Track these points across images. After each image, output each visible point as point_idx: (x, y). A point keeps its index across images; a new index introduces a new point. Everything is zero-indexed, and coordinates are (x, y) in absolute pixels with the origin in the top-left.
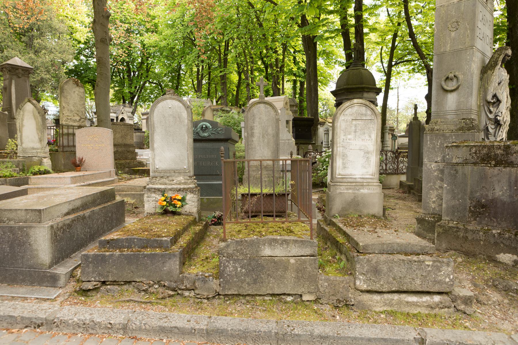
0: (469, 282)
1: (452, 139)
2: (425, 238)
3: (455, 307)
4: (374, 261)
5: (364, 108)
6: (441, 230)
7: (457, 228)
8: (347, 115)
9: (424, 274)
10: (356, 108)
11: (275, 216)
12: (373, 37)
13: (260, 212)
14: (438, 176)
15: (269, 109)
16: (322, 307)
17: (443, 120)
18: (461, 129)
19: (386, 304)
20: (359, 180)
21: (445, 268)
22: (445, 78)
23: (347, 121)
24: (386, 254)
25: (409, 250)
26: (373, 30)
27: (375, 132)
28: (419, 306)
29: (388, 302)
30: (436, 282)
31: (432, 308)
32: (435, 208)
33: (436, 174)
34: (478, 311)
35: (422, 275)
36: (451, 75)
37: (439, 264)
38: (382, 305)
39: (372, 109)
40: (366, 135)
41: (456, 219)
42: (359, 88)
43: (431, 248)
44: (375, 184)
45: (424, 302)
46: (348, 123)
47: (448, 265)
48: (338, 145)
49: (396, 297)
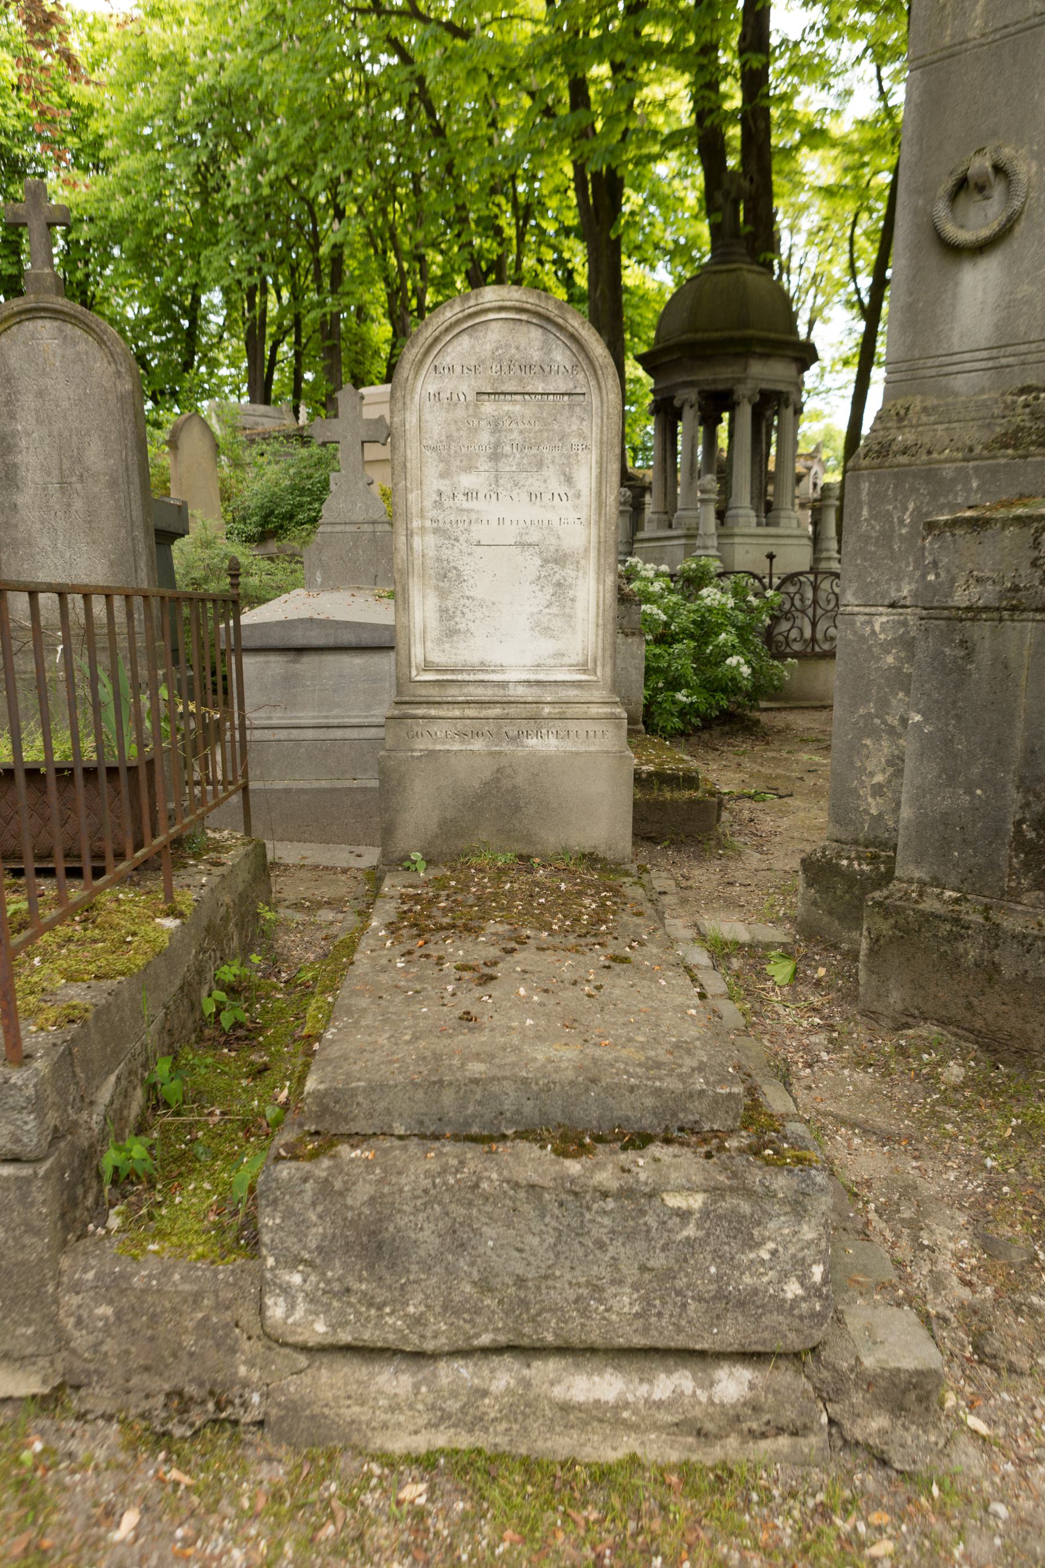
0: (962, 1219)
1: (969, 490)
2: (835, 947)
3: (831, 1422)
4: (362, 1192)
5: (536, 334)
6: (885, 927)
7: (957, 921)
9: (659, 1261)
10: (494, 335)
12: (817, 167)
14: (899, 670)
15: (82, 347)
16: (73, 1445)
17: (932, 401)
18: (1011, 440)
19: (441, 1419)
20: (521, 691)
21: (779, 1224)
22: (948, 183)
24: (456, 1138)
26: (815, 136)
27: (594, 457)
28: (633, 1428)
29: (453, 1406)
30: (725, 1301)
32: (880, 816)
33: (890, 659)
34: (974, 1422)
35: (643, 1268)
36: (981, 164)
37: (745, 1208)
38: (422, 1421)
39: (573, 337)
40: (551, 473)
41: (953, 879)
42: (731, 342)
43: (717, 1100)
44: (594, 710)
45: (659, 1405)
46: (460, 413)
47: (798, 1207)
48: (416, 523)
49: (502, 1377)
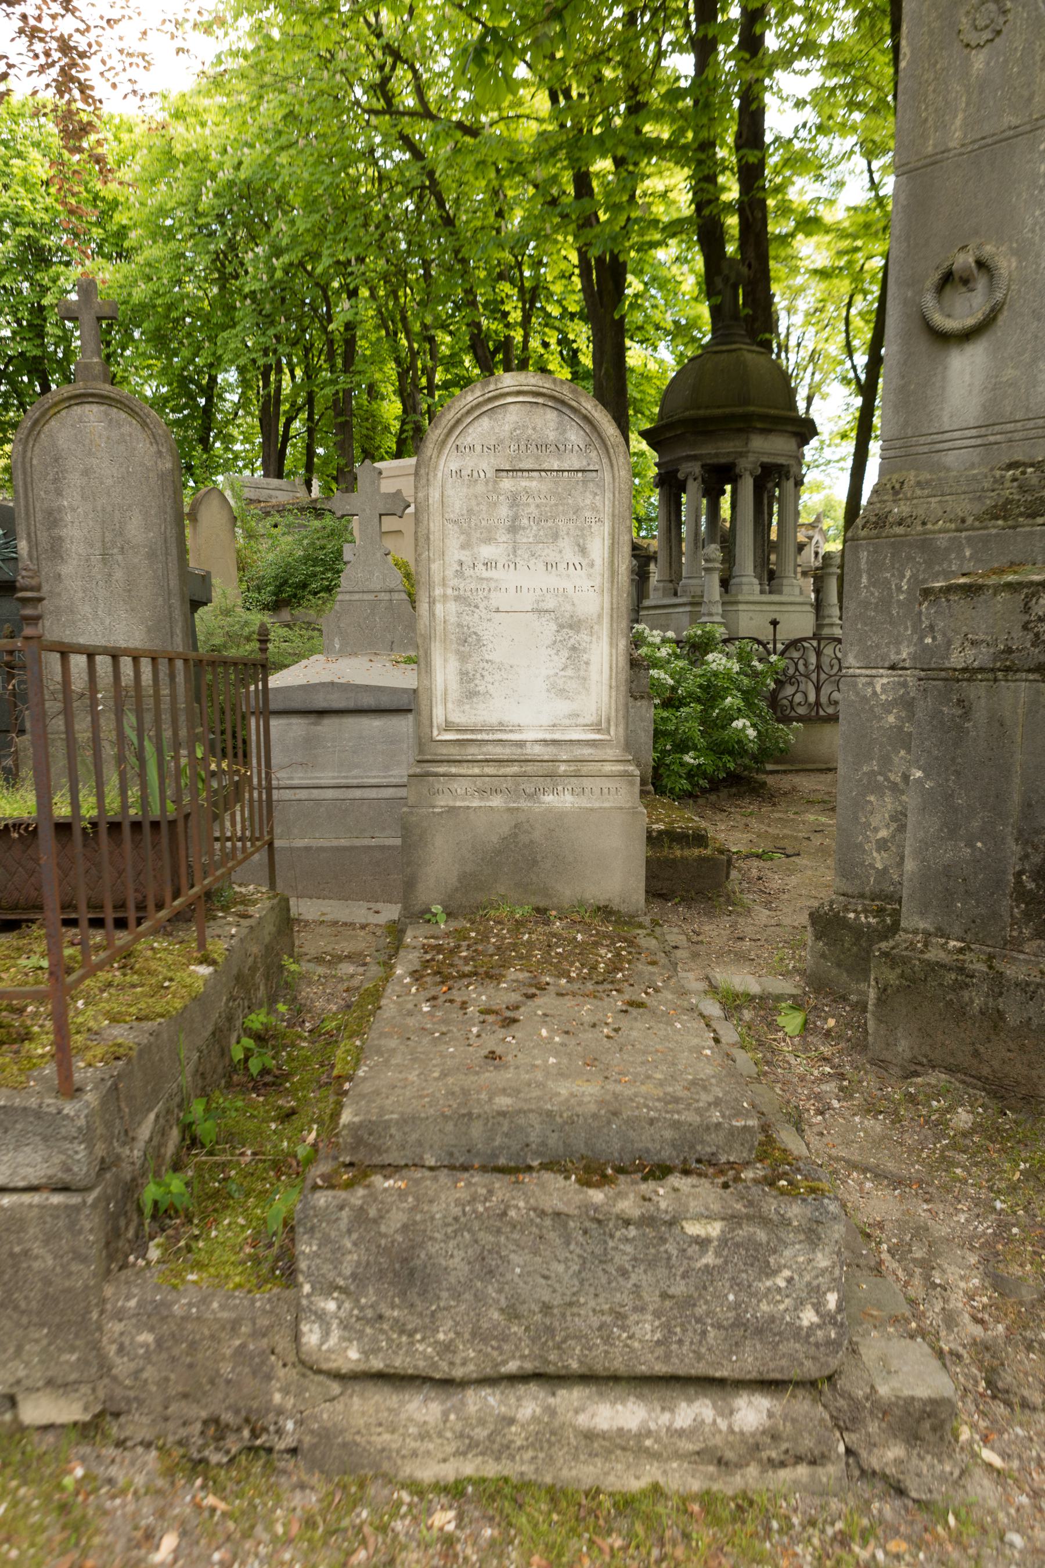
0: (973, 1259)
1: (962, 558)
2: (844, 999)
3: (849, 1451)
4: (397, 1218)
5: (551, 416)
6: (892, 977)
7: (961, 970)
8: (472, 448)
9: (679, 1288)
10: (513, 417)
11: (110, 922)
12: (812, 251)
13: (39, 908)
14: (900, 729)
15: (126, 429)
16: (113, 1471)
17: (925, 476)
18: (1001, 511)
19: (469, 1447)
20: (538, 750)
21: (794, 1253)
22: (935, 277)
23: (473, 479)
24: (484, 1169)
25: (611, 1146)
26: (809, 224)
27: (607, 528)
28: (655, 1456)
29: (481, 1433)
30: (744, 1329)
31: (720, 1462)
32: (885, 870)
33: (891, 719)
34: (988, 1455)
35: (664, 1296)
36: (965, 260)
37: (762, 1236)
38: (450, 1449)
39: (586, 419)
40: (566, 544)
41: (957, 930)
42: (732, 417)
43: (732, 1132)
44: (608, 768)
45: (681, 1433)
46: (480, 488)
47: (812, 1235)
48: (438, 592)
49: (528, 1405)
